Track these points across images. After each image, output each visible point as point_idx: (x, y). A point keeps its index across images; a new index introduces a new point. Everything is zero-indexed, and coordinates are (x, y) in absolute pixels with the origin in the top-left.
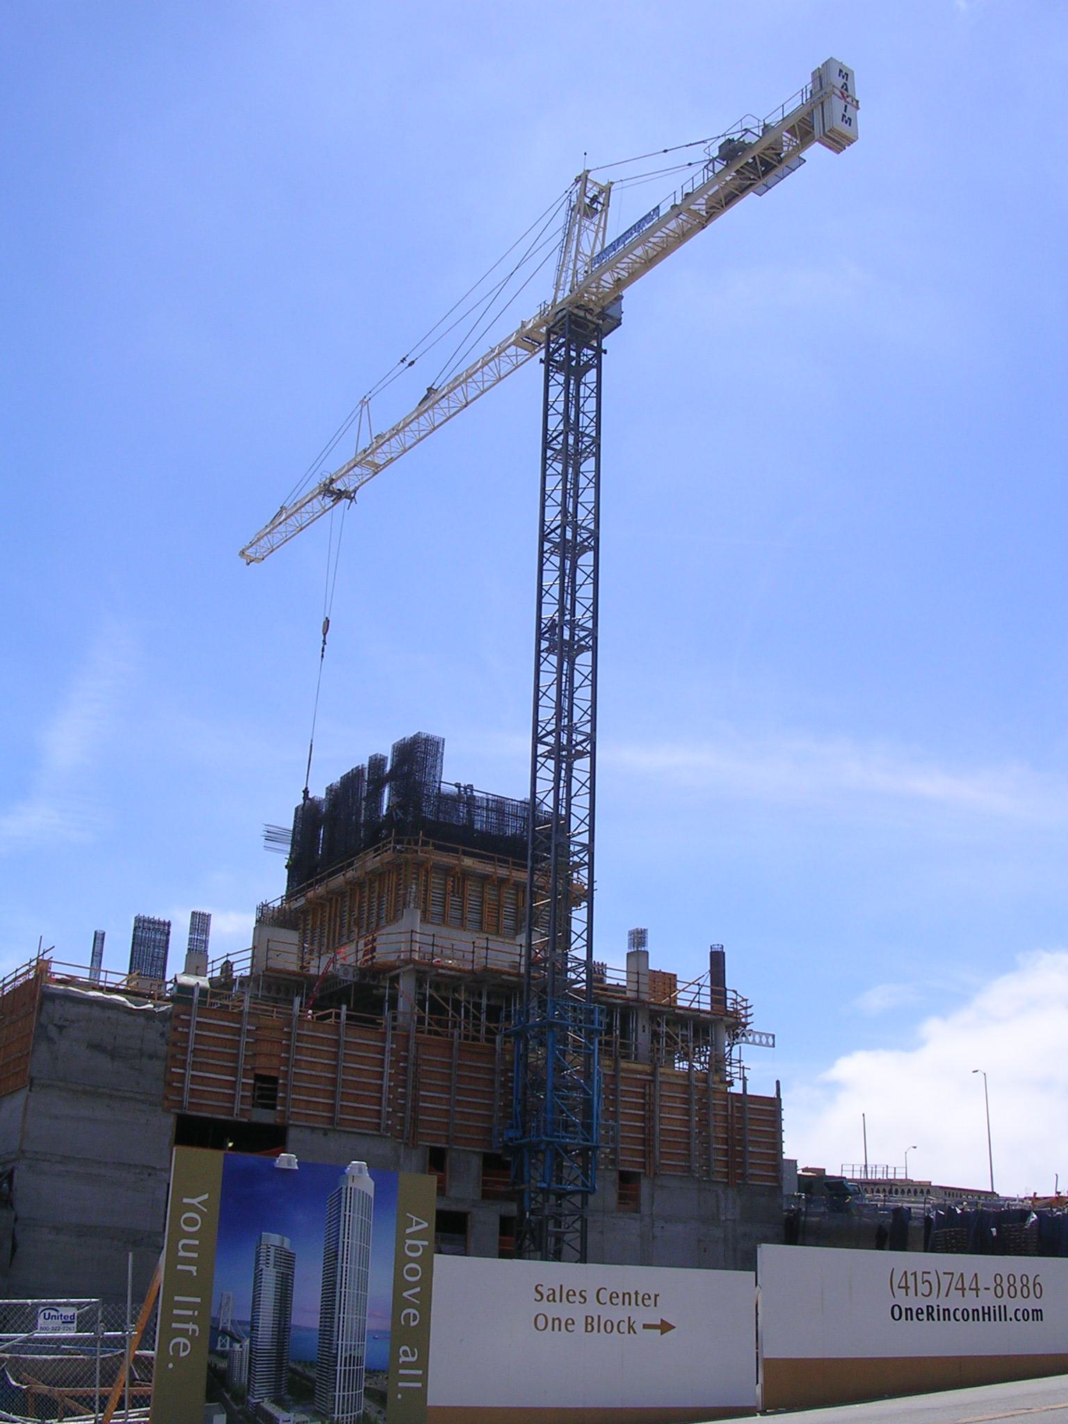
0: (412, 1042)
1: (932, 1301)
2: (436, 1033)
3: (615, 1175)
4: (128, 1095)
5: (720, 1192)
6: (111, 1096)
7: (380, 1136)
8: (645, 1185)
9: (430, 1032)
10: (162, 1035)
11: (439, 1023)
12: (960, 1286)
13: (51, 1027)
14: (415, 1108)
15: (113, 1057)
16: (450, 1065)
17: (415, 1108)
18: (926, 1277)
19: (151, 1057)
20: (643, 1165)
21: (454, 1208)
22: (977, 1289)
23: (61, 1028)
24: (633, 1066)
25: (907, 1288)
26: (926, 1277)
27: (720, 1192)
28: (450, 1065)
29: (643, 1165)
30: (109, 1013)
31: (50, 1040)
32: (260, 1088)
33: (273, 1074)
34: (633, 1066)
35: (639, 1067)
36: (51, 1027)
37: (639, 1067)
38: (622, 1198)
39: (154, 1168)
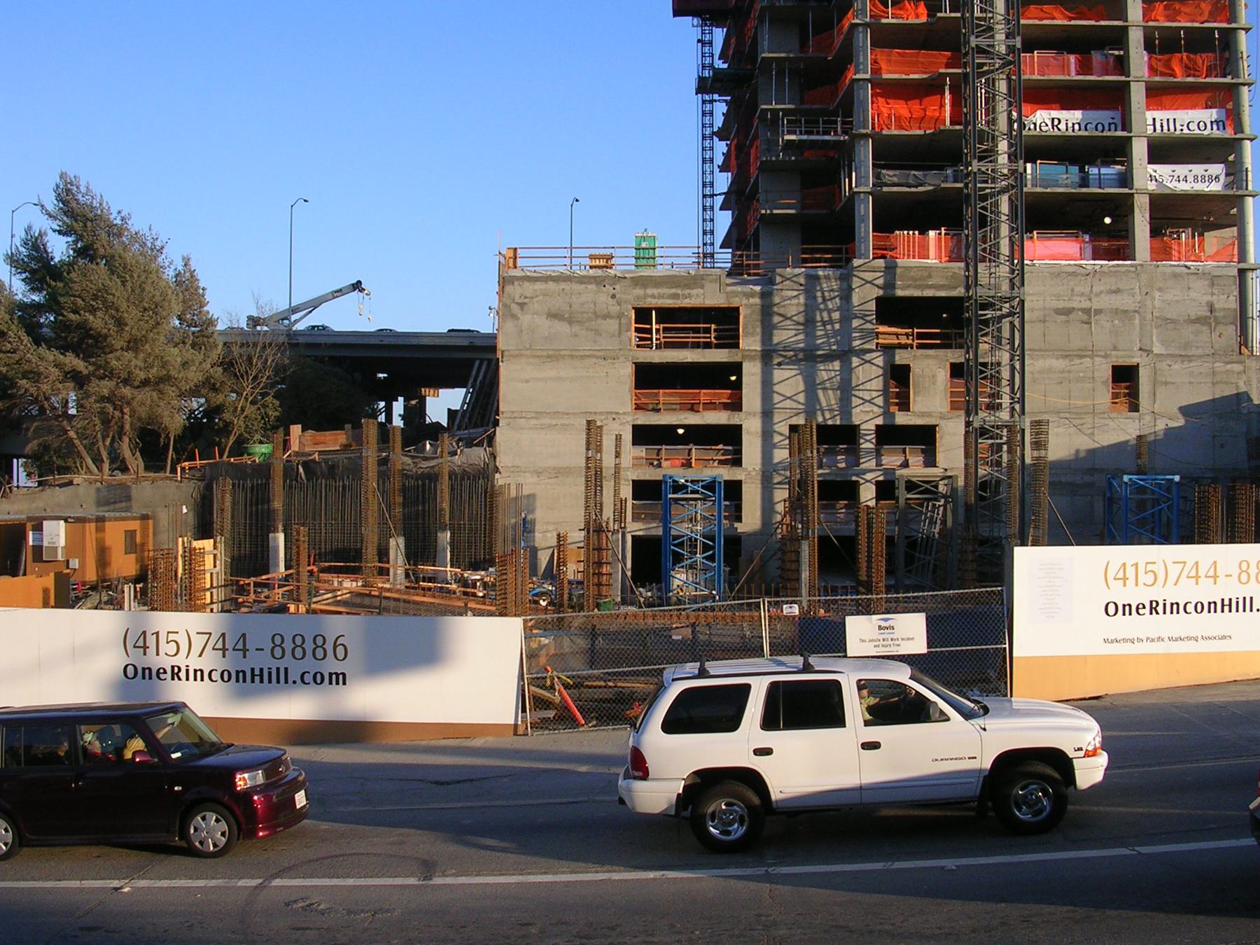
1: (180, 660)
4: (587, 353)
6: (572, 357)
10: (613, 296)
12: (220, 645)
13: (514, 306)
15: (570, 321)
18: (171, 637)
19: (605, 317)
21: (919, 422)
22: (245, 650)
23: (522, 305)
25: (145, 647)
26: (171, 637)
30: (563, 285)
31: (514, 317)
32: (721, 330)
36: (514, 306)
39: (617, 413)
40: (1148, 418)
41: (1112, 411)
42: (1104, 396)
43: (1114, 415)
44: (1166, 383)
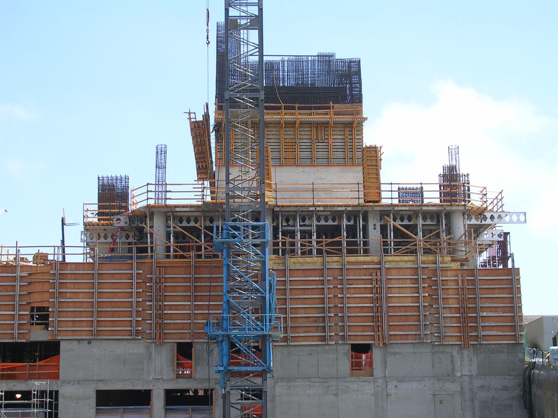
0: (154, 267)
2: (182, 257)
3: (348, 348)
5: (455, 353)
7: (134, 339)
8: (377, 354)
9: (176, 257)
11: (183, 248)
14: (160, 316)
16: (188, 280)
17: (160, 316)
20: (373, 337)
24: (361, 259)
27: (455, 353)
28: (188, 280)
29: (373, 337)
33: (45, 305)
34: (361, 259)
35: (368, 259)
37: (368, 259)
38: (356, 366)
40: (380, 381)
41: (352, 375)
42: (345, 364)
43: (354, 379)
44: (395, 354)
